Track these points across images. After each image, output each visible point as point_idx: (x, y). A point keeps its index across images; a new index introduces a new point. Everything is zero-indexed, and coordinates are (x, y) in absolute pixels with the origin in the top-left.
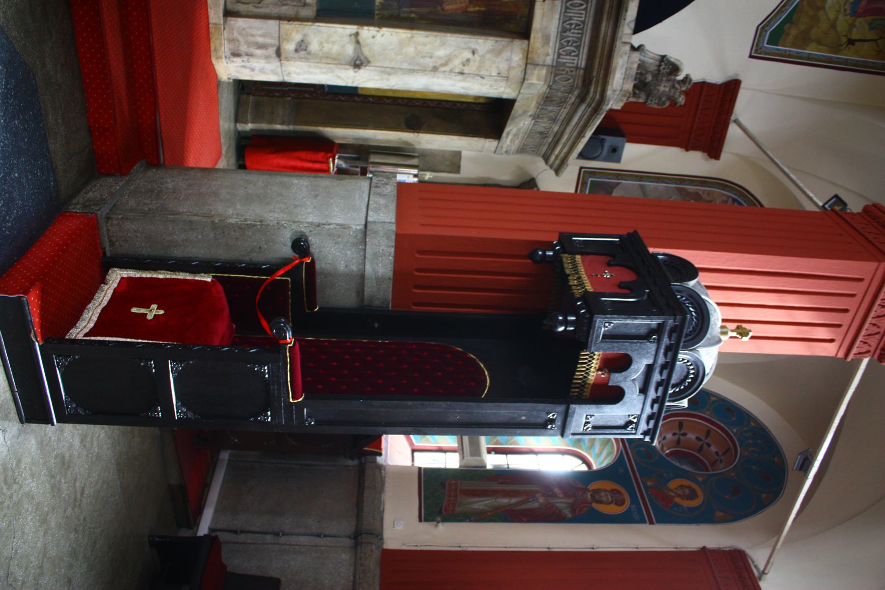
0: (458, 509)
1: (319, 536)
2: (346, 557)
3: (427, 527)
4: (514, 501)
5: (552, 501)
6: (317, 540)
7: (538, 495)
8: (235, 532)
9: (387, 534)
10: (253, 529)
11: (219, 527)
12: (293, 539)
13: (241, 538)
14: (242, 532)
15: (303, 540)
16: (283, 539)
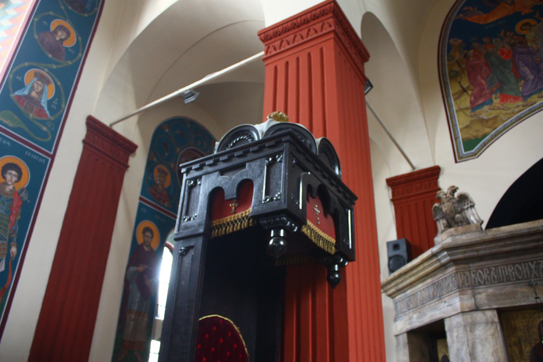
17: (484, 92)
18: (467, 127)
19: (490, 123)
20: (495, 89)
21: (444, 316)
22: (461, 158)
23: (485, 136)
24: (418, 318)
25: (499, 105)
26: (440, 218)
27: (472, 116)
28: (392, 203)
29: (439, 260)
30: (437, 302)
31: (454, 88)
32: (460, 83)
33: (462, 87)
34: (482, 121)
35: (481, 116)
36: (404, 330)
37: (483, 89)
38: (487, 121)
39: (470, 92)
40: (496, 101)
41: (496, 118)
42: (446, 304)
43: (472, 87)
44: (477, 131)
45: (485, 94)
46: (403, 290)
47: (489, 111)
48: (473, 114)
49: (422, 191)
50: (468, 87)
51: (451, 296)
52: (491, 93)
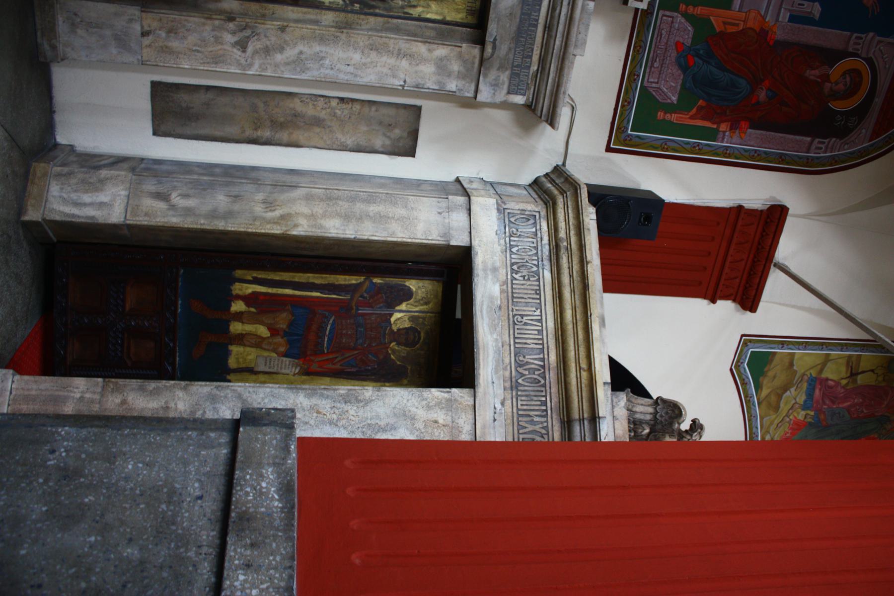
17: (827, 402)
18: (791, 364)
19: (773, 398)
20: (822, 417)
21: (480, 390)
22: (745, 344)
23: (758, 387)
24: (491, 298)
25: (791, 417)
26: (656, 412)
27: (804, 374)
28: (735, 205)
29: (581, 420)
30: (507, 374)
31: (868, 358)
32: (872, 371)
33: (863, 372)
34: (785, 389)
35: (793, 390)
36: (475, 243)
37: (833, 403)
38: (780, 397)
39: (844, 382)
40: (801, 415)
41: (777, 408)
42: (499, 406)
43: (850, 386)
44: (775, 377)
45: (824, 403)
46: (554, 258)
47: (793, 402)
48: (806, 378)
49: (726, 270)
50: (855, 381)
51: (509, 421)
52: (819, 411)
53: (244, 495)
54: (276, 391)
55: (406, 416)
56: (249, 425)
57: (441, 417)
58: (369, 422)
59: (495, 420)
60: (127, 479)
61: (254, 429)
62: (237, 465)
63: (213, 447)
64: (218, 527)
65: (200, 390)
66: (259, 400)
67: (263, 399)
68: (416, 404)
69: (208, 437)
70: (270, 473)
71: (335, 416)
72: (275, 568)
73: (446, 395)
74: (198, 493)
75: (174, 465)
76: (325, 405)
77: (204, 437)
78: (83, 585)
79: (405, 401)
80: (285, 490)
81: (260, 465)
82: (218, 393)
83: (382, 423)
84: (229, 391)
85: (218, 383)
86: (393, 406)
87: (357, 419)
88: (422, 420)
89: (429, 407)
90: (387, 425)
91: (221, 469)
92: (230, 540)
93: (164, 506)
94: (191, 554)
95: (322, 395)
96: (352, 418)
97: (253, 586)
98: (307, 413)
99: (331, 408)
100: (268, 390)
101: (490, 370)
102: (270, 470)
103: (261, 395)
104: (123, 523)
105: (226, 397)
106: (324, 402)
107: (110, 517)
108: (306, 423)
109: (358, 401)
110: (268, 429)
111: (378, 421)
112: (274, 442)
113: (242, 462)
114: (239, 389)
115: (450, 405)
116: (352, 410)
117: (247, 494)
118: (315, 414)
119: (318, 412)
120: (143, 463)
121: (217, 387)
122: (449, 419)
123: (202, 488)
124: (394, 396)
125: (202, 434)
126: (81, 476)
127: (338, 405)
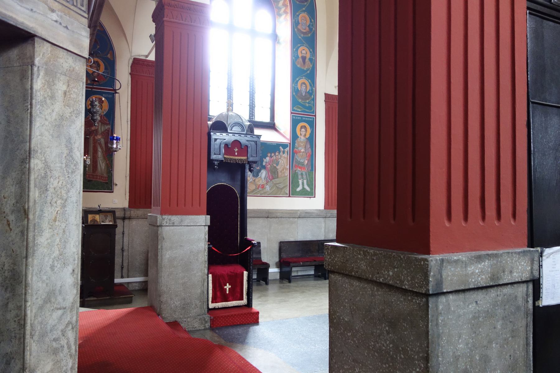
0: (105, 175)
1: (123, 234)
2: (134, 222)
3: (116, 189)
4: (100, 150)
5: (100, 132)
6: (126, 235)
7: (96, 138)
8: (122, 268)
9: (120, 206)
10: (121, 261)
11: (120, 275)
12: (126, 243)
13: (125, 264)
14: (122, 265)
15: (126, 240)
16: (126, 248)
21: (39, 31)
42: (54, 16)
51: (67, 10)
53: (482, 281)
54: (36, 268)
55: (60, 125)
56: (442, 287)
57: (61, 87)
58: (64, 165)
59: (66, 27)
60: (467, 344)
61: (444, 283)
62: (467, 287)
63: (449, 304)
64: (489, 290)
65: (34, 354)
66: (45, 285)
67: (43, 282)
68: (49, 111)
69: (442, 309)
70: (470, 269)
71: (59, 202)
72: (512, 260)
73: (42, 73)
74: (474, 304)
75: (460, 323)
76: (49, 213)
77: (442, 312)
78: (510, 339)
79: (47, 123)
80: (479, 259)
81: (466, 275)
82: (37, 334)
83: (66, 152)
84: (36, 322)
85: (28, 336)
86: (51, 137)
87: (61, 178)
88: (63, 107)
89: (52, 97)
90: (67, 146)
91: (461, 296)
92: (501, 282)
93: (480, 319)
94: (500, 298)
95: (40, 217)
96: (60, 183)
97: (518, 269)
98: (56, 231)
99: (52, 206)
100: (35, 278)
101: (19, 8)
102: (469, 269)
103: (40, 284)
104: (488, 335)
105: (41, 323)
106: (46, 215)
107: (485, 343)
108: (64, 231)
109: (45, 177)
110: (444, 274)
111: (64, 156)
112: (452, 269)
113: (465, 286)
114: (34, 311)
115: (51, 74)
116: (54, 183)
117: (482, 279)
118: (57, 223)
119: (55, 220)
120: (459, 340)
121: (32, 336)
122: (62, 78)
123: (472, 303)
124: (41, 135)
125: (441, 313)
126: (466, 368)
127: (49, 198)
